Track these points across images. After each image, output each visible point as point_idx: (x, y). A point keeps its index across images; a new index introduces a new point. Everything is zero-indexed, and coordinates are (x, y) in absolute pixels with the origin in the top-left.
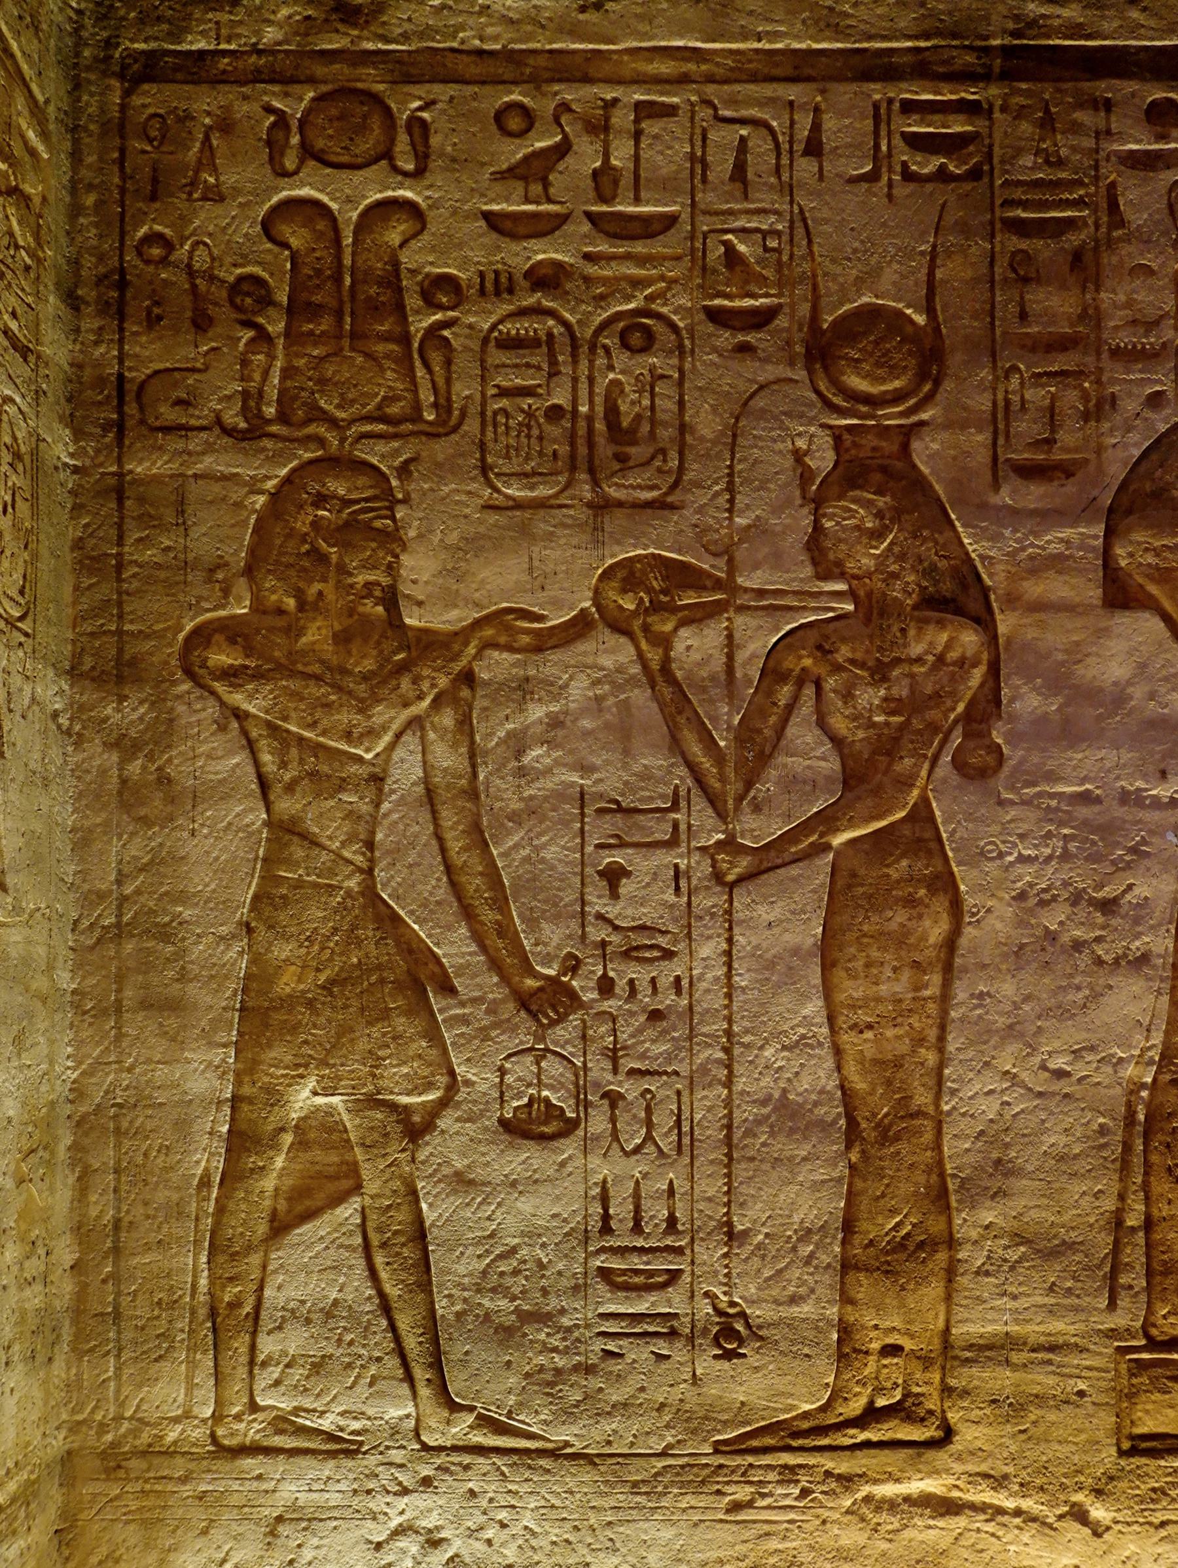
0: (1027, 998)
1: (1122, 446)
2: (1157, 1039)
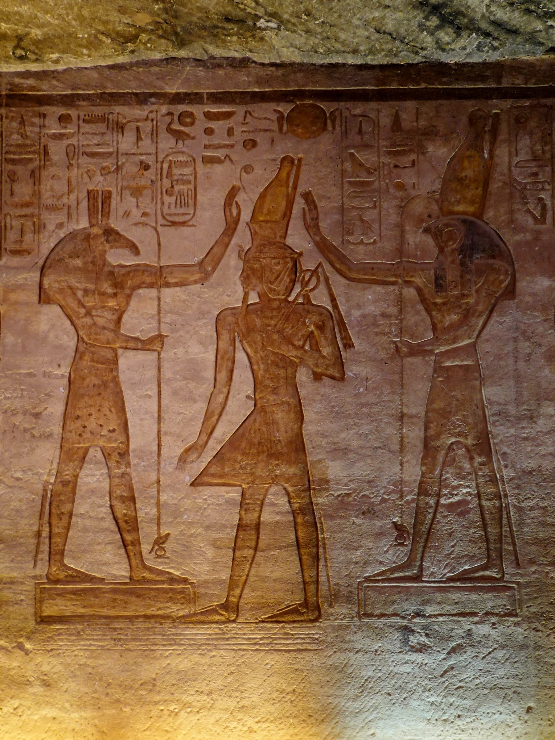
0: (5, 451)
1: (48, 243)
2: (55, 466)
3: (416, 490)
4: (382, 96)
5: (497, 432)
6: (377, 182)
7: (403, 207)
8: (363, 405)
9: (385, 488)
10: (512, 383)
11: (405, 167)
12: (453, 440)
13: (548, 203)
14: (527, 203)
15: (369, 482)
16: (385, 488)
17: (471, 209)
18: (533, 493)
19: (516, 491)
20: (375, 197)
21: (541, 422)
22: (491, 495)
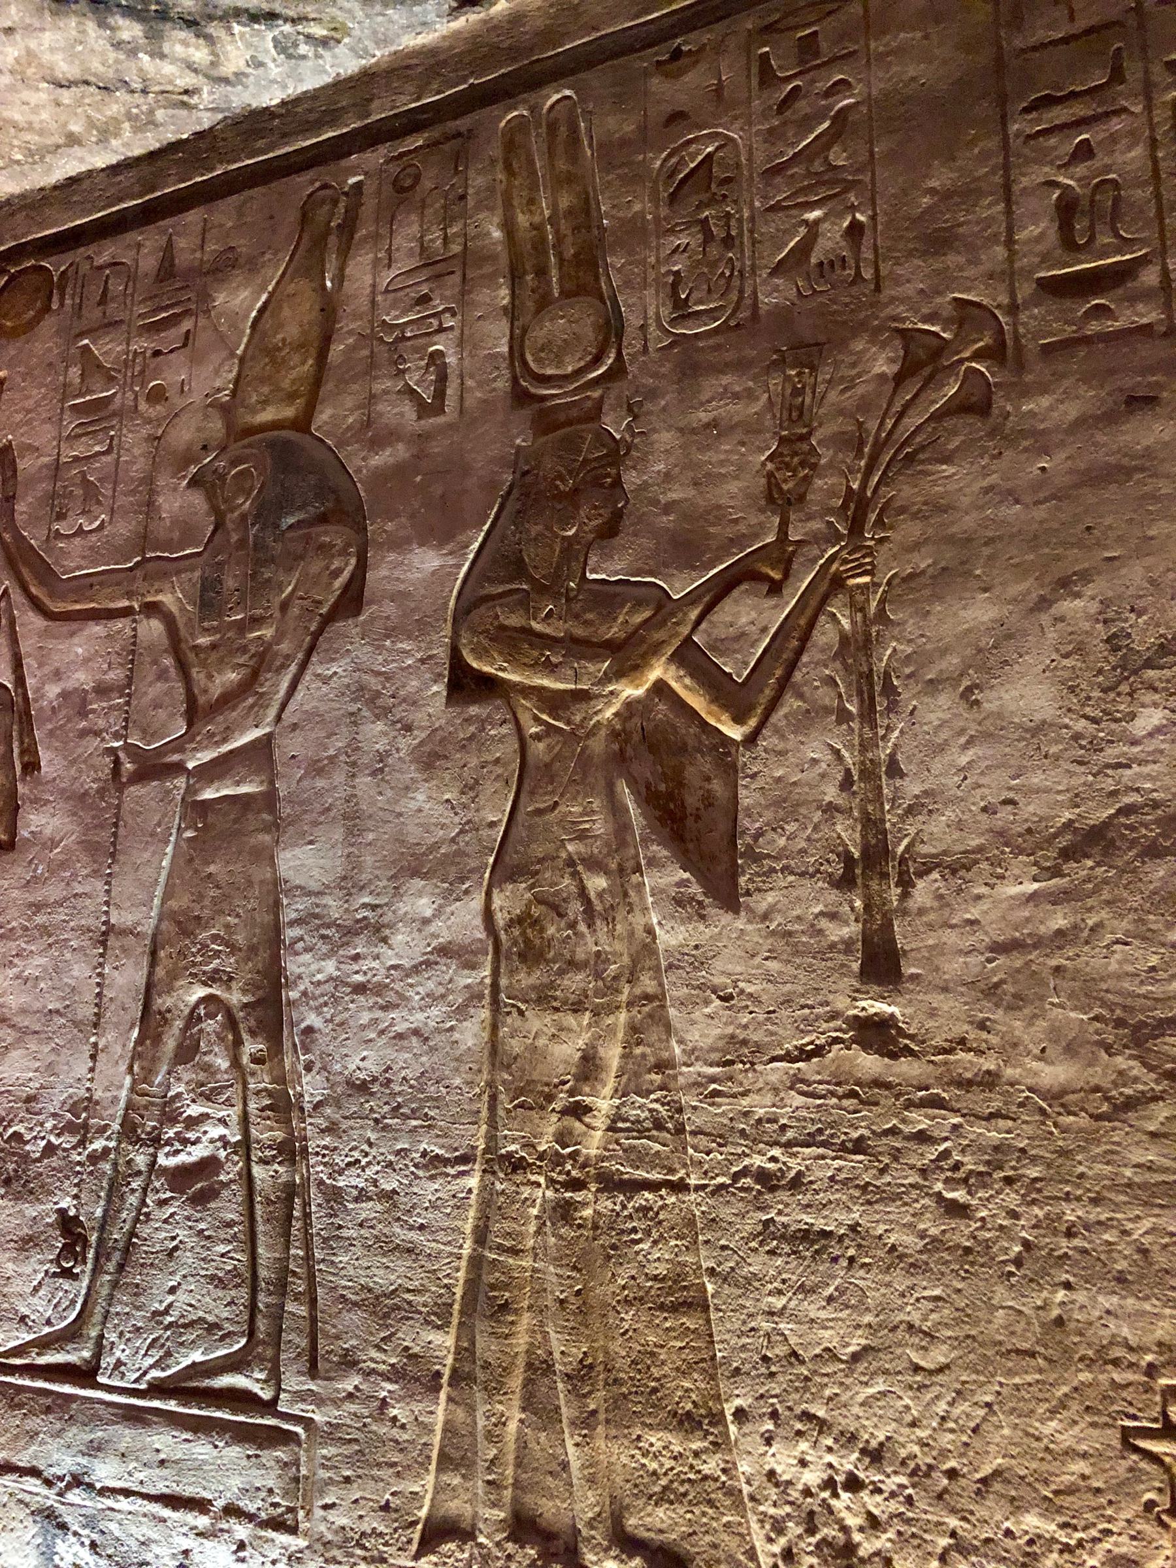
3: (116, 1126)
4: (149, 214)
5: (298, 971)
6: (119, 396)
7: (159, 438)
8: (38, 907)
9: (54, 1115)
10: (338, 834)
11: (171, 351)
12: (201, 992)
13: (451, 360)
14: (404, 371)
15: (29, 1099)
16: (54, 1115)
17: (289, 412)
18: (365, 1147)
19: (327, 1141)
20: (112, 428)
21: (398, 939)
22: (270, 1147)
